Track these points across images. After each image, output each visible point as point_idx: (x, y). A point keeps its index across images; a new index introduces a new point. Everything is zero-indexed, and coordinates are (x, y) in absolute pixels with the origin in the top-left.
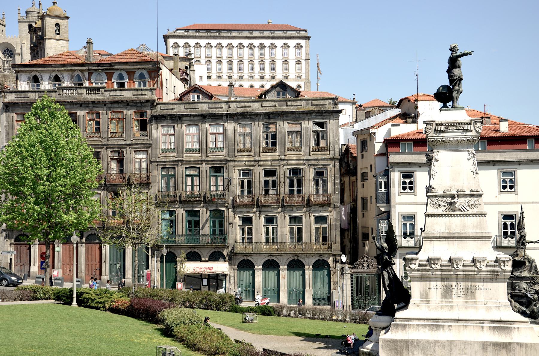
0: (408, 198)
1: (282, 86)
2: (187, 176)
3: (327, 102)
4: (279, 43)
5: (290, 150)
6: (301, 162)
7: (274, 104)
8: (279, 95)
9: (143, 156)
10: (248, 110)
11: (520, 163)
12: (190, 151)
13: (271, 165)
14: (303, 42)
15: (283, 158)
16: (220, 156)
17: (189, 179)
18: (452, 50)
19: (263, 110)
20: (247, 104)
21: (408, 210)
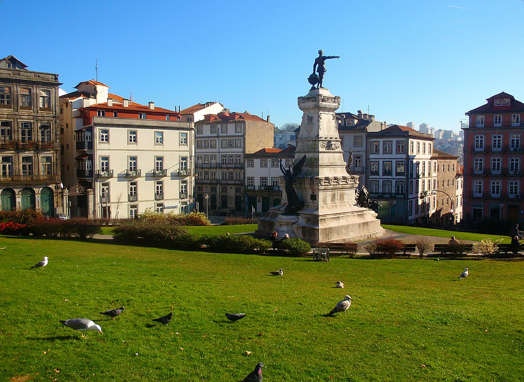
0: (104, 146)
3: (50, 77)
5: (22, 108)
6: (31, 117)
7: (9, 72)
8: (9, 66)
13: (7, 118)
15: (17, 113)
18: (320, 52)
21: (105, 154)
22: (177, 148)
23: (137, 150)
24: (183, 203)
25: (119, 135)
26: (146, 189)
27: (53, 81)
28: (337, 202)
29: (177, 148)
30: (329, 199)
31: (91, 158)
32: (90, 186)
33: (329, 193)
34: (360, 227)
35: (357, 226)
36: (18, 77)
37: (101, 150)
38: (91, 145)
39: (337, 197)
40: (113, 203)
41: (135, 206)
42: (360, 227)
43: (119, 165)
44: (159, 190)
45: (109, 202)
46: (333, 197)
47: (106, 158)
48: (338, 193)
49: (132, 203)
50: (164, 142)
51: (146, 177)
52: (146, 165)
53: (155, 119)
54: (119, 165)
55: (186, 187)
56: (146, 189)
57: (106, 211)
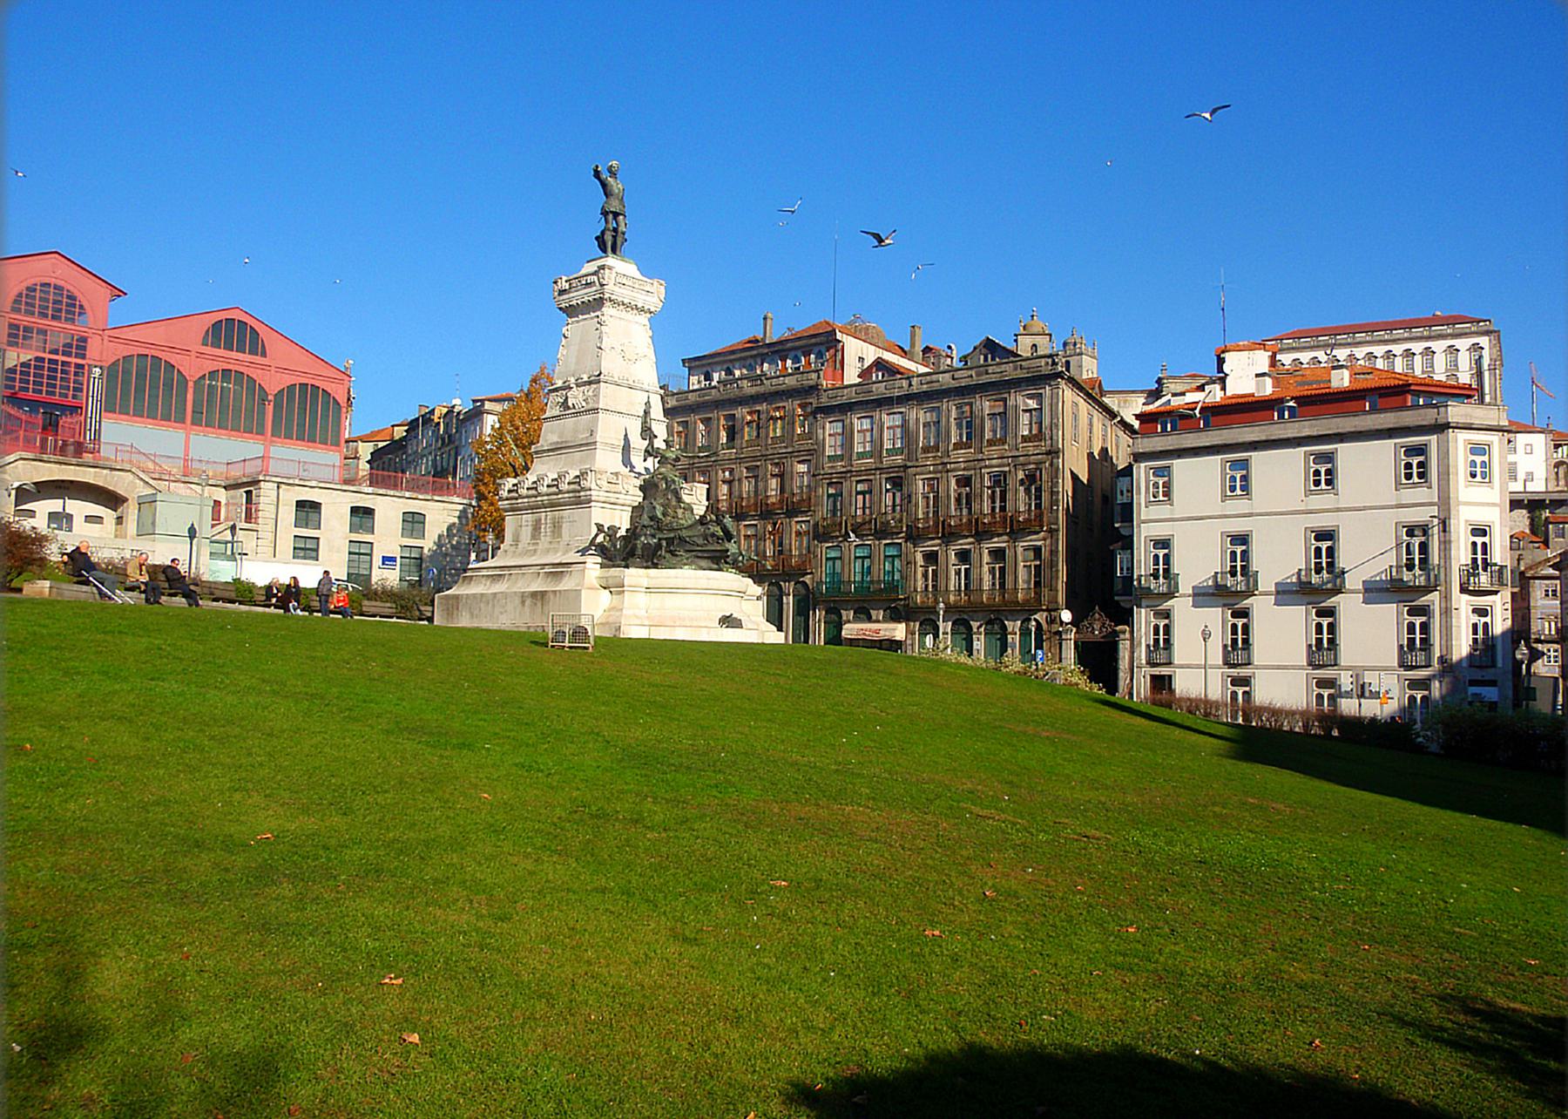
0: (1162, 511)
1: (990, 347)
2: (858, 493)
3: (1043, 362)
4: (1439, 346)
5: (991, 443)
9: (802, 468)
10: (936, 386)
11: (1341, 437)
12: (861, 456)
14: (1484, 341)
16: (899, 460)
17: (860, 497)
19: (954, 384)
20: (934, 377)
21: (1160, 531)
22: (1391, 496)
23: (1251, 515)
24: (1414, 684)
25: (1198, 478)
26: (1281, 633)
27: (1047, 370)
28: (544, 541)
29: (1391, 496)
30: (526, 533)
31: (1128, 543)
32: (1126, 617)
33: (528, 518)
34: (523, 602)
35: (517, 601)
36: (985, 379)
37: (1149, 522)
38: (1127, 512)
39: (546, 529)
40: (1181, 667)
41: (1244, 681)
42: (523, 602)
43: (1198, 562)
44: (1325, 636)
45: (1169, 664)
46: (537, 527)
47: (1164, 543)
48: (546, 516)
49: (1234, 672)
50: (1340, 481)
51: (1278, 593)
52: (1280, 557)
53: (1337, 414)
54: (1198, 562)
55: (1425, 627)
56: (1281, 633)
57: (1161, 684)
